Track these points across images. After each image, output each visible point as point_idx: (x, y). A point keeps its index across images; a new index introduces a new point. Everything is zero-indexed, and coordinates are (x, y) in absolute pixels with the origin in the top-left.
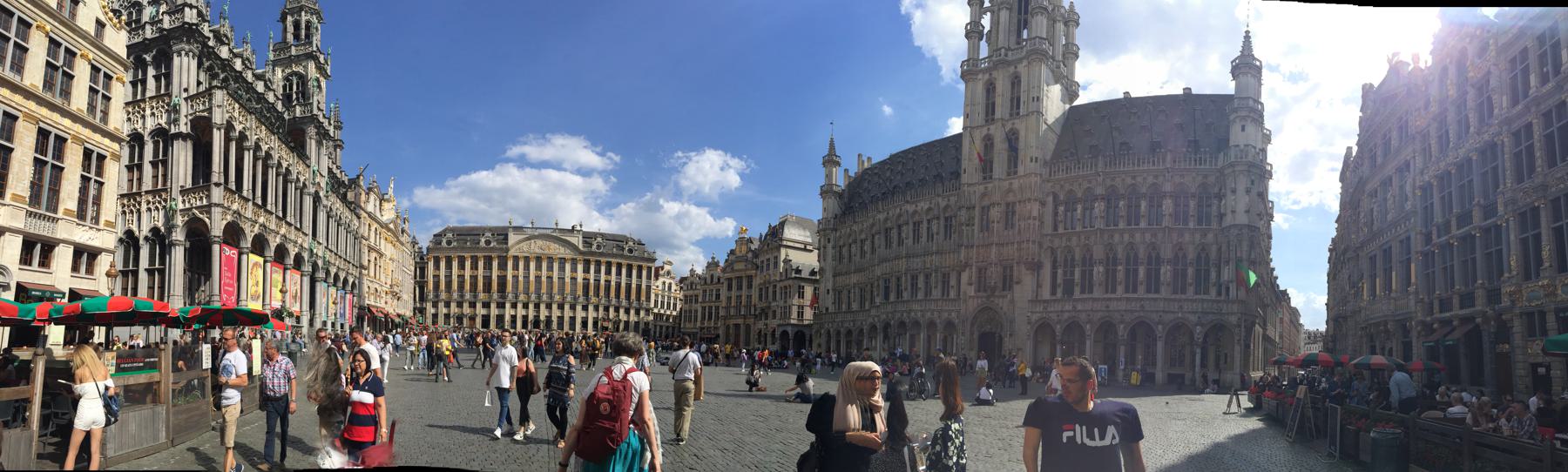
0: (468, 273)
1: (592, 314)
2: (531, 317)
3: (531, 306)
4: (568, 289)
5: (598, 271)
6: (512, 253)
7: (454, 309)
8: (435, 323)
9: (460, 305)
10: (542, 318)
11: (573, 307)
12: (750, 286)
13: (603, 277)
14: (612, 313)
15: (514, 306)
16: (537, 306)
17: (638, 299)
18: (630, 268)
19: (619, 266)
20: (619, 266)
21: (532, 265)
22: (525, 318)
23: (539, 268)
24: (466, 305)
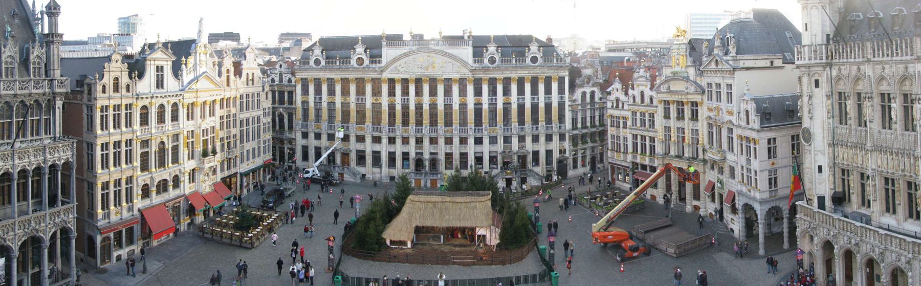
2: (412, 155)
12: (695, 117)
13: (500, 99)
15: (392, 141)
16: (419, 141)
18: (534, 82)
19: (521, 82)
20: (521, 82)
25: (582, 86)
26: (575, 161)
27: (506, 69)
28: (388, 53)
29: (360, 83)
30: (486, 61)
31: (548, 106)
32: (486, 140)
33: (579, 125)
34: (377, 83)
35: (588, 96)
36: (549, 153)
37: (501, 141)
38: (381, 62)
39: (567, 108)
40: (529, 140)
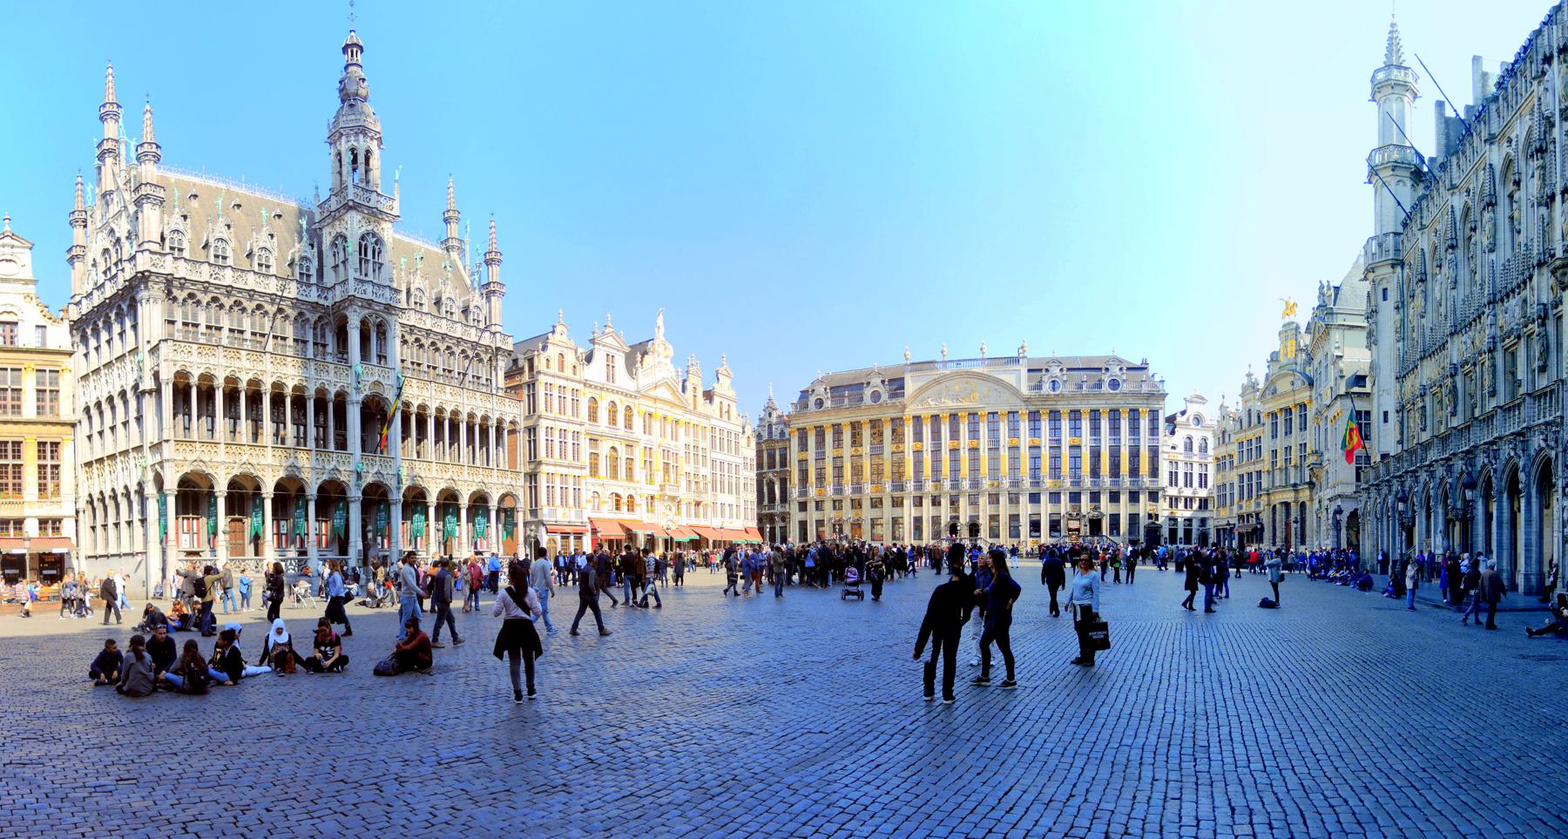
1: (1045, 509)
3: (945, 502)
4: (1005, 465)
5: (1055, 429)
6: (911, 411)
9: (837, 505)
10: (964, 520)
11: (1014, 500)
13: (1066, 439)
14: (1085, 505)
15: (918, 502)
16: (954, 502)
17: (1134, 472)
18: (1115, 415)
21: (945, 430)
22: (936, 520)
23: (955, 434)
26: (1173, 532)
34: (897, 423)
38: (903, 395)
40: (1104, 498)
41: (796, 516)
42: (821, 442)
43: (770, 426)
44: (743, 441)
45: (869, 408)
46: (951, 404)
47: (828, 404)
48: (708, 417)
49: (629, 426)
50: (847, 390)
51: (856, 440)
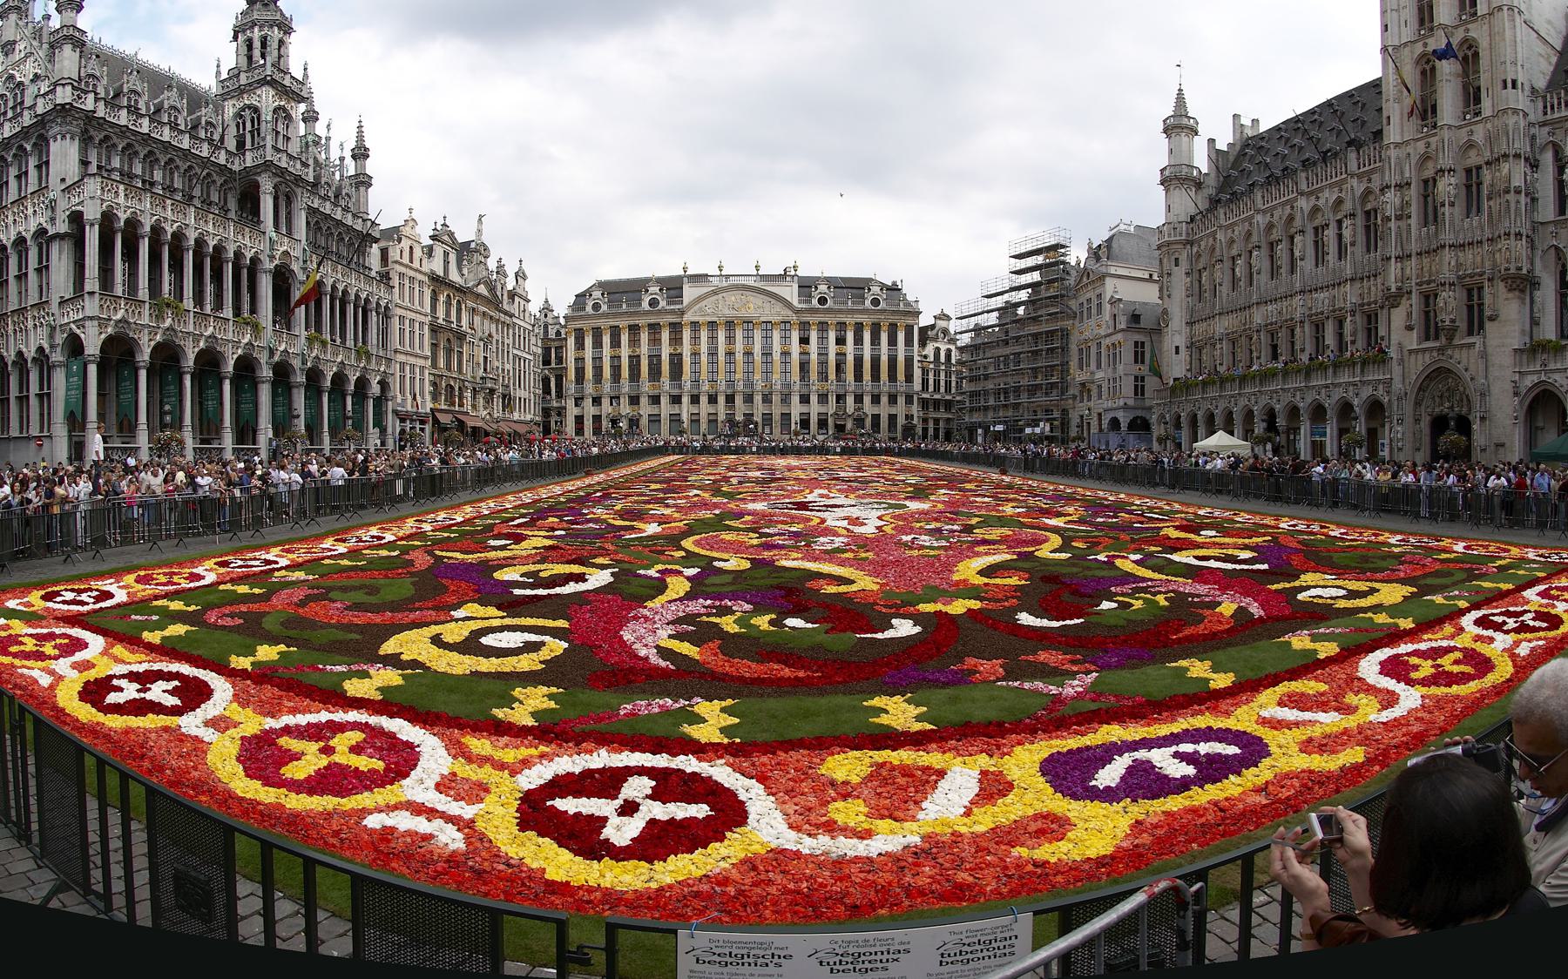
0: (625, 352)
1: (815, 408)
5: (823, 339)
6: (689, 317)
7: (606, 408)
8: (580, 430)
10: (739, 418)
11: (786, 399)
15: (695, 399)
16: (730, 399)
19: (859, 328)
20: (859, 328)
23: (730, 339)
24: (624, 401)
25: (935, 339)
26: (925, 430)
27: (840, 311)
28: (689, 293)
29: (654, 328)
30: (815, 302)
31: (893, 361)
32: (814, 398)
33: (931, 389)
34: (676, 328)
35: (943, 354)
36: (892, 418)
37: (832, 399)
39: (916, 364)
40: (867, 400)
41: (572, 411)
42: (598, 344)
43: (546, 327)
44: (533, 340)
45: (646, 313)
46: (728, 313)
47: (604, 308)
48: (511, 316)
49: (459, 319)
50: (622, 292)
51: (634, 342)
